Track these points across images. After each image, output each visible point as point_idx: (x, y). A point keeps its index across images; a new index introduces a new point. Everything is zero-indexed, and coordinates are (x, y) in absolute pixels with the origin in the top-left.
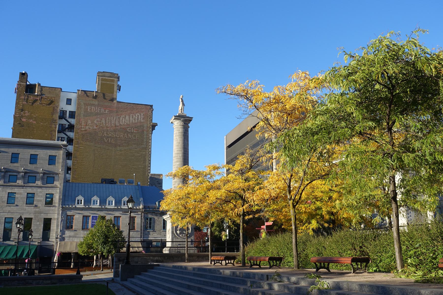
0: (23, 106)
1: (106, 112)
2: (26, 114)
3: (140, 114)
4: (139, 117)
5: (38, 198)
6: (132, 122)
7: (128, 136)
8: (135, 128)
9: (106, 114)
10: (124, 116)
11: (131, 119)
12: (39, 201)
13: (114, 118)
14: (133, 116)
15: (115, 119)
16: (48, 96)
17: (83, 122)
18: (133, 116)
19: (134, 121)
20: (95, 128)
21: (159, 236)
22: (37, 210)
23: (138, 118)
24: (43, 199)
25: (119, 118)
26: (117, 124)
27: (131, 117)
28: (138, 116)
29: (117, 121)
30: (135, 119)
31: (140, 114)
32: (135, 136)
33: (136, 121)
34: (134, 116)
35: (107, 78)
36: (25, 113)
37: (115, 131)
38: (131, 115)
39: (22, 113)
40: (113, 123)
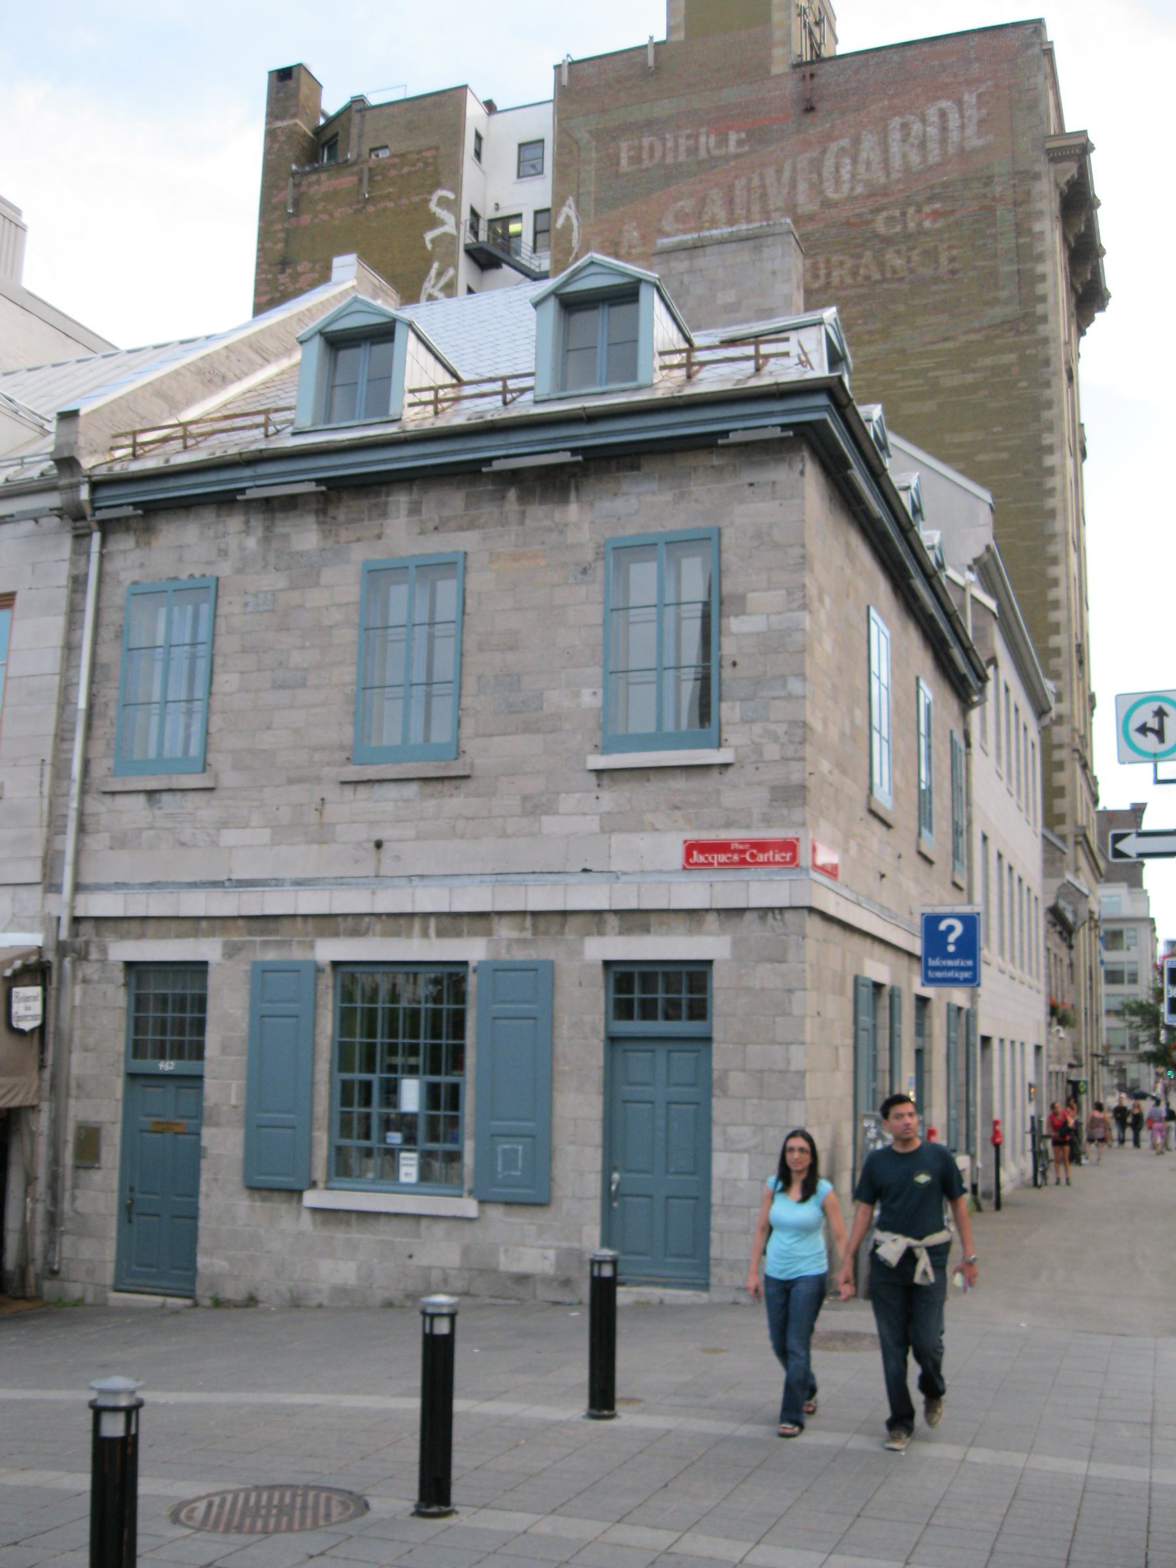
0: (286, 241)
3: (960, 103)
4: (954, 121)
6: (907, 169)
7: (881, 266)
8: (931, 199)
9: (727, 158)
11: (895, 148)
13: (779, 172)
14: (905, 126)
15: (787, 174)
16: (403, 147)
18: (905, 126)
19: (915, 158)
21: (300, 858)
23: (944, 129)
25: (816, 165)
26: (805, 203)
27: (896, 135)
28: (943, 114)
29: (802, 186)
30: (923, 145)
31: (960, 103)
32: (930, 255)
33: (934, 156)
34: (916, 128)
38: (896, 122)
39: (283, 278)
40: (777, 200)
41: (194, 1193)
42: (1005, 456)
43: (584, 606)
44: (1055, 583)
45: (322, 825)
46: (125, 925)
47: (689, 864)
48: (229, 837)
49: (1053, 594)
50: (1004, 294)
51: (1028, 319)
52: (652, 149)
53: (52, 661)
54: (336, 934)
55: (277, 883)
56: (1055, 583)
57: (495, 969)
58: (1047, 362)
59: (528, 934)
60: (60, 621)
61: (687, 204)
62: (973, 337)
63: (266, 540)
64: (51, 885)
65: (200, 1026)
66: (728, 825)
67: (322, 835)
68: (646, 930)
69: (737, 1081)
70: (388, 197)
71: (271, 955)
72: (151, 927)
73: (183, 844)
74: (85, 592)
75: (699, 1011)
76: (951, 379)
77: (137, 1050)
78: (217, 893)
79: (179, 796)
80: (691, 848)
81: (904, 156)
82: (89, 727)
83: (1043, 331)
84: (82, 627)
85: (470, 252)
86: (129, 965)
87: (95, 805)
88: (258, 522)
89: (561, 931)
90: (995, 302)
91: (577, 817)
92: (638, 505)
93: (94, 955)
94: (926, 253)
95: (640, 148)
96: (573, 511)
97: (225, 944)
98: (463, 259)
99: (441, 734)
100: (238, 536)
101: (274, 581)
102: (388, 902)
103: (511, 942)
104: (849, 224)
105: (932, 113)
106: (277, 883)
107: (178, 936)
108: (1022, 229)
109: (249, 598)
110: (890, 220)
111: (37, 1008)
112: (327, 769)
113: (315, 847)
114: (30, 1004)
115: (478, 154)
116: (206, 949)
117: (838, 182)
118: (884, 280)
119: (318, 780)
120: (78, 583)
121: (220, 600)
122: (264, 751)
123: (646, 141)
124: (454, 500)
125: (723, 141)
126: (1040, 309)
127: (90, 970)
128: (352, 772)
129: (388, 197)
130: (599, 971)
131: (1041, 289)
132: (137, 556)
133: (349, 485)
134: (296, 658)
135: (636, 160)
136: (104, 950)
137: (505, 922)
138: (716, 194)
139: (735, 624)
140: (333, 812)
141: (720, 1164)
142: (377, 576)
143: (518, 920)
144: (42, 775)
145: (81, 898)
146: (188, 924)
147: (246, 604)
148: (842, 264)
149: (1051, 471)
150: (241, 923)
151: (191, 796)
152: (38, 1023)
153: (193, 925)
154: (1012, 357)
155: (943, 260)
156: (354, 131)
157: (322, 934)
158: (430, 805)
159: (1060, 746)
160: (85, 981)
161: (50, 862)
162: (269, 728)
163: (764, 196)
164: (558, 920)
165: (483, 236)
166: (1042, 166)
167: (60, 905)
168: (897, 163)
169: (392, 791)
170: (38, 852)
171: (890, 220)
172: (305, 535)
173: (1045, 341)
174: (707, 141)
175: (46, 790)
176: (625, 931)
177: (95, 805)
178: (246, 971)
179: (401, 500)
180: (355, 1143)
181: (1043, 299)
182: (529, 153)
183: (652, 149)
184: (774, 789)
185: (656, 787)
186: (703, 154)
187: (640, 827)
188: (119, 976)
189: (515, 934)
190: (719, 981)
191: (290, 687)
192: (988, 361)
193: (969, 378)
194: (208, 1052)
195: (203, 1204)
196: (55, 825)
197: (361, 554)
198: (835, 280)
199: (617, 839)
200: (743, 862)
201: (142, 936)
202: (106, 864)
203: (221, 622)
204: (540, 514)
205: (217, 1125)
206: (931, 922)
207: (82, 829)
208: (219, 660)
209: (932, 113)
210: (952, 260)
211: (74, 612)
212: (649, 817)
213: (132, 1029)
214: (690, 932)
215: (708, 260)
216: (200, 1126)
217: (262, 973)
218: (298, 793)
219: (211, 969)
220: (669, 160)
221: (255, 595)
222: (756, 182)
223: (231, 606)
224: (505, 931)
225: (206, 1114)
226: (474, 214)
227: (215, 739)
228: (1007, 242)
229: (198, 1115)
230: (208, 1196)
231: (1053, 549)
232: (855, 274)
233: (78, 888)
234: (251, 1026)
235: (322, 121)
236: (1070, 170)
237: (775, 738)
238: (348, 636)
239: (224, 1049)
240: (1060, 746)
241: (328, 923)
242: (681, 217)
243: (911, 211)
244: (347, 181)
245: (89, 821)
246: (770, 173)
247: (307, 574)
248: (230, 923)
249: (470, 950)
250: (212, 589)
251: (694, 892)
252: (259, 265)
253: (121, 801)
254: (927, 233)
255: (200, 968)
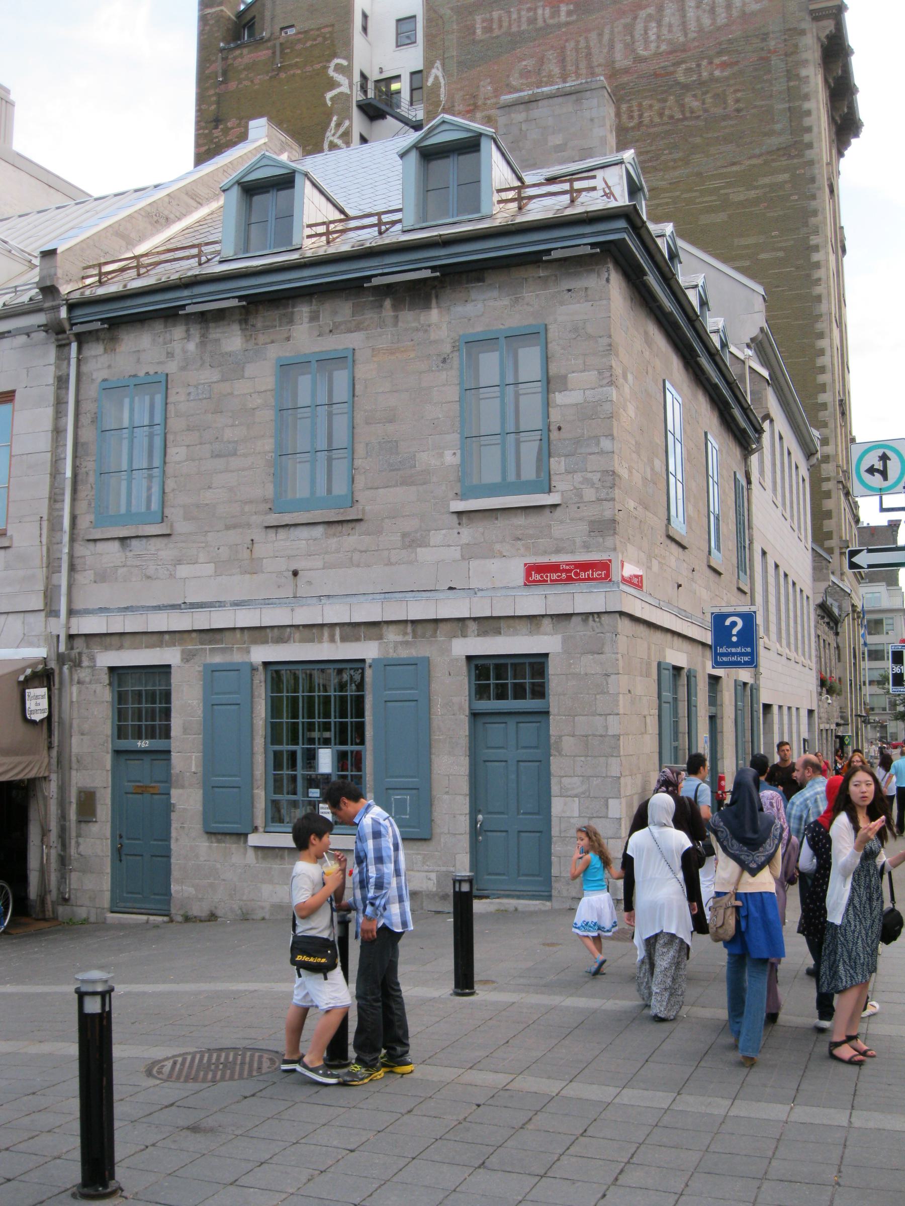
0: (218, 103)
1: (563, 18)
6: (701, 30)
7: (682, 106)
8: (720, 53)
9: (559, 26)
10: (651, 10)
11: (691, 14)
13: (600, 35)
15: (606, 37)
19: (706, 21)
21: (238, 586)
25: (629, 29)
26: (621, 60)
29: (619, 47)
30: (712, 10)
32: (720, 98)
33: (722, 19)
39: (217, 133)
40: (599, 58)
41: (167, 838)
42: (781, 254)
43: (445, 387)
44: (822, 352)
45: (252, 559)
46: (108, 639)
47: (529, 582)
48: (183, 571)
49: (820, 361)
50: (778, 127)
51: (797, 146)
52: (500, 20)
53: (44, 442)
54: (265, 642)
55: (220, 604)
56: (822, 352)
57: (386, 664)
58: (813, 180)
59: (409, 638)
60: (50, 411)
61: (529, 63)
62: (754, 161)
63: (202, 344)
64: (51, 611)
65: (167, 713)
66: (558, 551)
67: (253, 567)
68: (498, 632)
69: (568, 744)
70: (296, 65)
71: (217, 659)
72: (127, 641)
73: (149, 577)
74: (67, 388)
75: (540, 692)
76: (739, 195)
77: (120, 732)
78: (175, 614)
79: (144, 540)
80: (531, 569)
81: (698, 19)
82: (74, 491)
83: (809, 154)
84: (66, 416)
85: (362, 107)
86: (112, 670)
87: (82, 550)
88: (196, 331)
89: (434, 635)
90: (771, 133)
91: (444, 548)
92: (485, 309)
93: (86, 663)
94: (716, 96)
95: (491, 20)
96: (434, 315)
97: (183, 652)
98: (355, 112)
99: (340, 488)
100: (181, 342)
101: (209, 375)
102: (303, 616)
103: (396, 644)
104: (656, 75)
106: (220, 604)
107: (148, 647)
108: (792, 75)
109: (191, 389)
110: (688, 70)
111: (44, 704)
112: (255, 517)
113: (248, 576)
114: (38, 701)
115: (365, 29)
116: (169, 656)
117: (646, 41)
118: (685, 119)
119: (249, 525)
120: (61, 382)
121: (169, 391)
122: (207, 505)
123: (495, 15)
124: (344, 309)
125: (556, 13)
126: (807, 138)
127: (83, 674)
128: (274, 519)
129: (296, 65)
130: (464, 662)
131: (807, 122)
132: (104, 360)
133: (262, 300)
134: (228, 434)
135: (488, 29)
136: (92, 659)
137: (392, 628)
138: (551, 55)
139: (559, 398)
140: (259, 550)
141: (557, 806)
142: (287, 369)
143: (401, 627)
144: (41, 529)
145: (74, 621)
146: (155, 638)
147: (189, 394)
148: (651, 106)
149: (817, 265)
150: (194, 635)
151: (154, 540)
152: (46, 715)
153: (159, 638)
154: (786, 176)
155: (730, 101)
156: (268, 14)
157: (255, 642)
158: (333, 542)
159: (828, 479)
160: (79, 682)
161: (50, 595)
162: (210, 488)
163: (589, 55)
164: (431, 626)
165: (371, 94)
166: (807, 24)
167: (58, 626)
168: (692, 26)
169: (304, 532)
170: (41, 587)
171: (688, 70)
172: (232, 340)
173: (811, 163)
174: (544, 13)
175: (44, 540)
176: (483, 633)
177: (82, 550)
178: (199, 671)
179: (303, 310)
180: (284, 798)
181: (809, 130)
182: (406, 27)
183: (500, 20)
184: (592, 523)
185: (502, 522)
186: (540, 23)
187: (491, 554)
188: (105, 678)
189: (400, 638)
190: (553, 668)
191: (225, 456)
192: (767, 180)
193: (752, 194)
194: (173, 733)
195: (173, 846)
196: (52, 566)
197: (274, 352)
198: (646, 120)
199: (474, 564)
200: (569, 579)
201: (121, 647)
202: (91, 594)
203: (171, 407)
204: (409, 318)
205: (183, 787)
206: (719, 619)
207: (72, 568)
208: (170, 437)
210: (737, 101)
211: (59, 404)
212: (497, 547)
213: (116, 718)
214: (531, 633)
215: (541, 111)
216: (169, 788)
217: (212, 672)
218: (233, 536)
219: (173, 670)
220: (514, 29)
221: (196, 387)
222: (582, 44)
223: (178, 396)
224: (392, 635)
225: (174, 778)
226: (363, 76)
227: (170, 497)
228: (780, 86)
229: (167, 780)
230: (177, 840)
231: (820, 326)
232: (661, 115)
233: (71, 612)
234: (204, 712)
235: (242, 7)
236: (829, 26)
237: (593, 485)
238: (267, 415)
239: (185, 730)
240: (828, 479)
241: (259, 634)
242: (525, 74)
243: (704, 63)
244: (263, 54)
245: (77, 561)
246: (593, 36)
247: (234, 369)
248: (186, 636)
249: (367, 650)
250: (165, 383)
251: (533, 602)
252: (198, 123)
253: (100, 546)
254: (717, 80)
255: (165, 670)
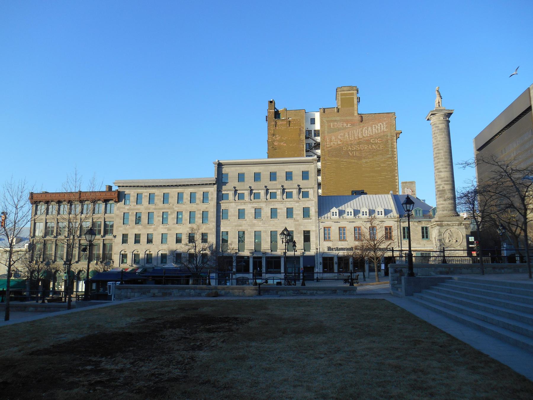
2: (277, 138)
4: (382, 127)
5: (297, 212)
11: (374, 129)
12: (297, 215)
16: (294, 118)
17: (328, 138)
19: (377, 132)
20: (339, 143)
22: (297, 223)
24: (301, 213)
25: (362, 131)
26: (361, 137)
32: (379, 147)
33: (379, 132)
35: (346, 92)
36: (276, 138)
37: (359, 144)
40: (356, 135)
61: (342, 134)
105: (379, 125)
125: (347, 125)
138: (346, 133)
174: (345, 125)
209: (379, 125)
228: (390, 146)
242: (341, 136)
247: (417, 227)
